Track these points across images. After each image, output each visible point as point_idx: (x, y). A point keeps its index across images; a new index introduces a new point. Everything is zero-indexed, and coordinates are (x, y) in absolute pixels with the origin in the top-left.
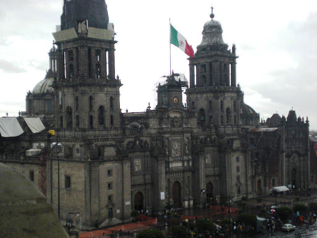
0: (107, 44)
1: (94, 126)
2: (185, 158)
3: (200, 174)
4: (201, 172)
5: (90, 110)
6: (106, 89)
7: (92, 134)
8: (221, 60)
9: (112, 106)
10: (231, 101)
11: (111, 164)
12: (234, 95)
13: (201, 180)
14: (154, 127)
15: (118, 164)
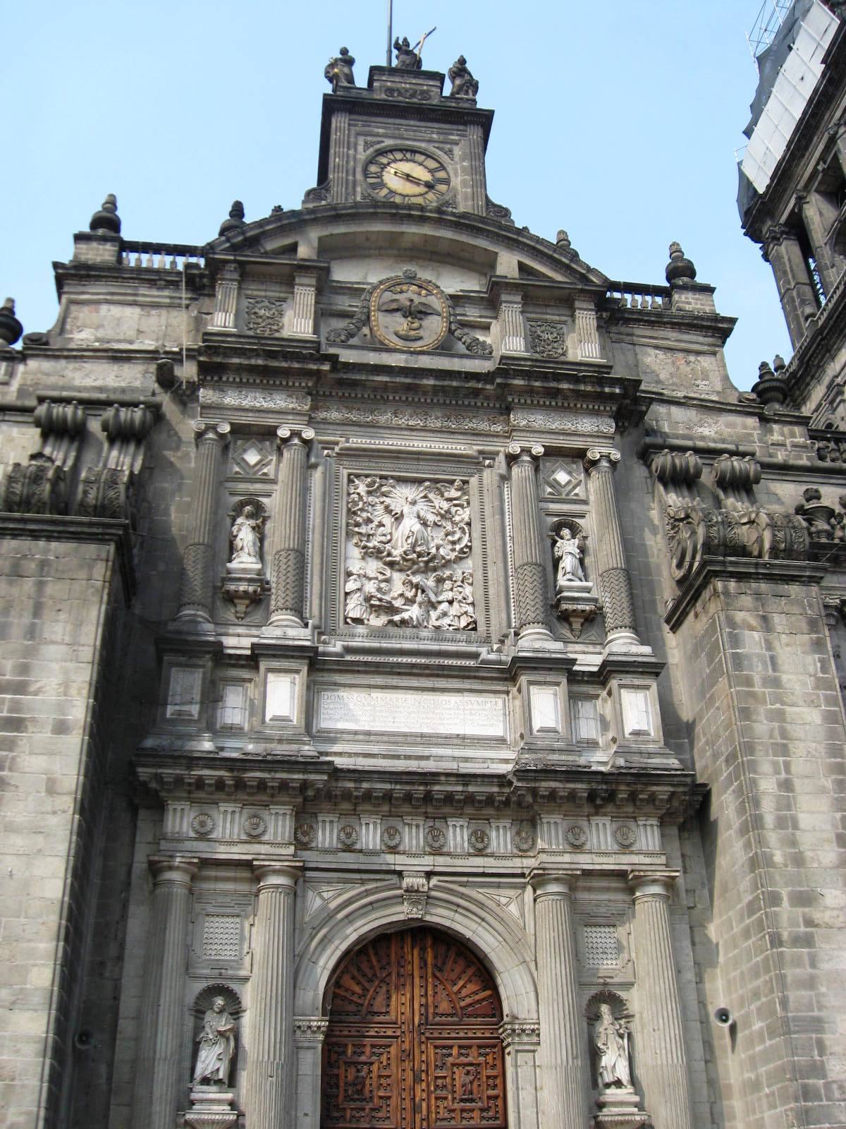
4: (787, 785)
13: (805, 899)
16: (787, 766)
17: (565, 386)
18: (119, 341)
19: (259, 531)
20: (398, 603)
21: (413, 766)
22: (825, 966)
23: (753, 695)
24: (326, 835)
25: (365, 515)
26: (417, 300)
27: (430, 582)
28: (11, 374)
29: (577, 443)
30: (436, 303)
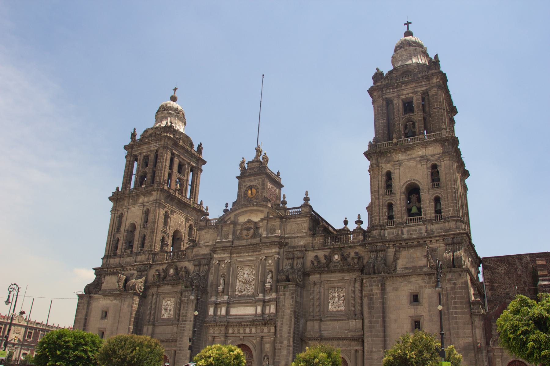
0: (158, 144)
1: (118, 251)
2: (261, 296)
3: (278, 329)
4: (282, 324)
5: (117, 231)
6: (141, 200)
7: (113, 263)
8: (388, 96)
9: (146, 221)
10: (419, 166)
11: (109, 302)
12: (434, 150)
13: (281, 343)
14: (207, 244)
15: (118, 302)
16: (283, 320)
17: (268, 244)
18: (207, 243)
19: (224, 280)
20: (243, 291)
21: (241, 320)
22: (282, 353)
23: (280, 308)
24: (230, 331)
25: (239, 274)
26: (249, 226)
27: (249, 286)
28: (192, 252)
29: (272, 255)
30: (252, 226)
